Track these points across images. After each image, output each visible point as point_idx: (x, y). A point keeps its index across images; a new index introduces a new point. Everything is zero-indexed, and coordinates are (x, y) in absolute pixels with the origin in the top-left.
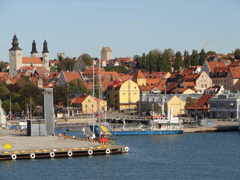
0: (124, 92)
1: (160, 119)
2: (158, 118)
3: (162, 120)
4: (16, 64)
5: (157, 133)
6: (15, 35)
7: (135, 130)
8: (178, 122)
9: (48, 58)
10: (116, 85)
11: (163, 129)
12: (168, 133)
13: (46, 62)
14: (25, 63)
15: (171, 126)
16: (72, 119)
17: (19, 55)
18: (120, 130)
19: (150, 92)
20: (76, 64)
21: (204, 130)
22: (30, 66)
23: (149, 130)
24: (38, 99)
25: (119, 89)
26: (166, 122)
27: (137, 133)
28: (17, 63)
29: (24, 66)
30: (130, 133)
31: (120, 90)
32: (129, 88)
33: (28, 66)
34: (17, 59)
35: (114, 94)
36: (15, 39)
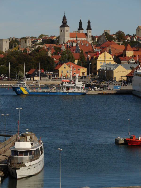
0: (101, 61)
1: (68, 83)
2: (66, 83)
3: (70, 84)
5: (64, 94)
6: (65, 16)
9: (91, 34)
10: (96, 56)
11: (70, 91)
12: (74, 94)
13: (89, 37)
14: (72, 38)
15: (77, 89)
17: (67, 31)
18: (36, 91)
19: (128, 62)
20: (100, 39)
21: (105, 93)
23: (59, 91)
24: (28, 65)
25: (97, 59)
26: (72, 86)
27: (49, 93)
28: (65, 37)
29: (71, 39)
30: (44, 94)
31: (98, 60)
32: (105, 58)
33: (74, 39)
34: (65, 34)
35: (94, 63)
36: (64, 18)
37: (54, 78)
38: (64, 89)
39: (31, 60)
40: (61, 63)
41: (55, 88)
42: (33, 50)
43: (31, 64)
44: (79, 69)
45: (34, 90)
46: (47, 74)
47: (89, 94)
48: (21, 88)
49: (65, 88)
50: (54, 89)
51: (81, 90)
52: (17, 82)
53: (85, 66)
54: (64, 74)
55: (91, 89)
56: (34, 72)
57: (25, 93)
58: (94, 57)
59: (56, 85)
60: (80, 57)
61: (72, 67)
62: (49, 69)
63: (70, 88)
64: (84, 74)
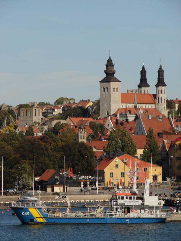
2: (125, 198)
3: (132, 200)
4: (110, 104)
5: (121, 222)
6: (110, 58)
7: (86, 215)
8: (157, 205)
9: (165, 95)
11: (132, 215)
12: (141, 221)
13: (162, 102)
15: (148, 211)
16: (75, 195)
17: (116, 89)
18: (61, 216)
22: (133, 107)
23: (110, 215)
26: (137, 204)
27: (88, 220)
28: (112, 103)
29: (124, 107)
33: (130, 107)
36: (110, 64)
37: (94, 187)
38: (119, 210)
39: (47, 151)
40: (108, 158)
41: (102, 209)
42: (46, 129)
43: (47, 158)
44: (146, 169)
45: (58, 214)
46: (81, 180)
47: (173, 219)
48: (30, 210)
49: (121, 209)
50: (99, 210)
51: (156, 212)
52: (18, 197)
53: (157, 163)
54: (114, 180)
55: (175, 211)
56: (53, 176)
57: (39, 221)
58: (177, 144)
59: (100, 202)
60: (147, 144)
61: (136, 164)
62: (83, 170)
63: (132, 209)
64: (156, 179)
